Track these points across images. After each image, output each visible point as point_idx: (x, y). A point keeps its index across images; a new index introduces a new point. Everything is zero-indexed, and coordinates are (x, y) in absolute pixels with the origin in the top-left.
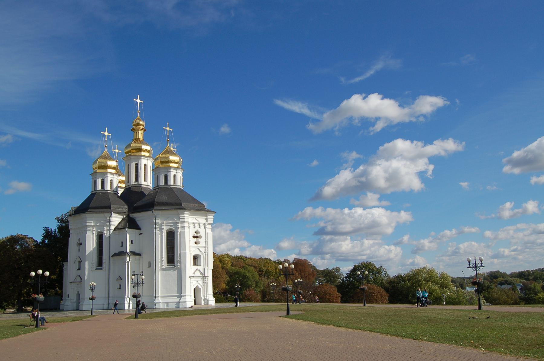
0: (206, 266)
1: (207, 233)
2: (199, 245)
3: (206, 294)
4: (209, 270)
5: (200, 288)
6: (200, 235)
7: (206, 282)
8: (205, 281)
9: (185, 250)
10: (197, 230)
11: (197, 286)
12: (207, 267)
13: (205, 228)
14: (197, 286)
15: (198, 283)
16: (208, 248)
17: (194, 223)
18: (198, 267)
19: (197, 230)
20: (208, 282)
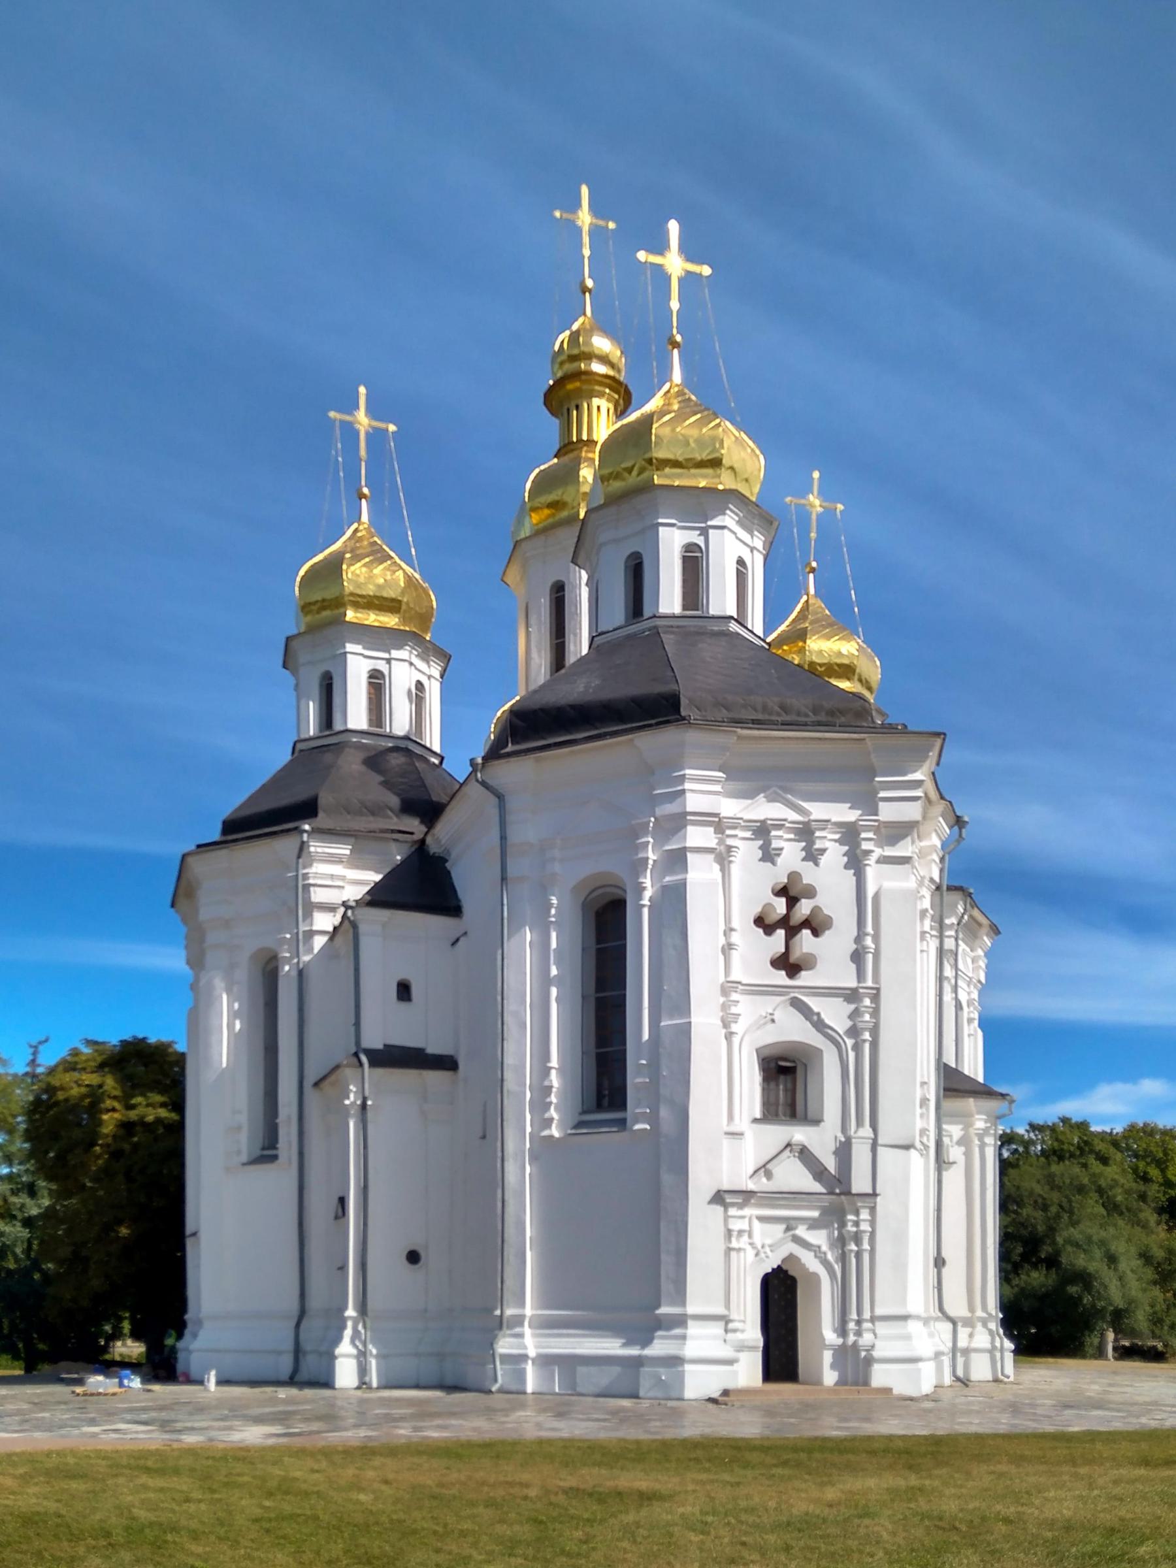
0: (860, 1123)
1: (876, 897)
2: (805, 978)
3: (859, 1313)
4: (880, 1150)
5: (814, 1278)
6: (816, 910)
7: (857, 1238)
8: (851, 1228)
9: (683, 1005)
10: (794, 876)
11: (791, 1258)
12: (866, 1131)
13: (856, 862)
14: (791, 1258)
15: (798, 1240)
16: (876, 997)
17: (762, 830)
18: (800, 1134)
19: (794, 876)
20: (873, 1234)
